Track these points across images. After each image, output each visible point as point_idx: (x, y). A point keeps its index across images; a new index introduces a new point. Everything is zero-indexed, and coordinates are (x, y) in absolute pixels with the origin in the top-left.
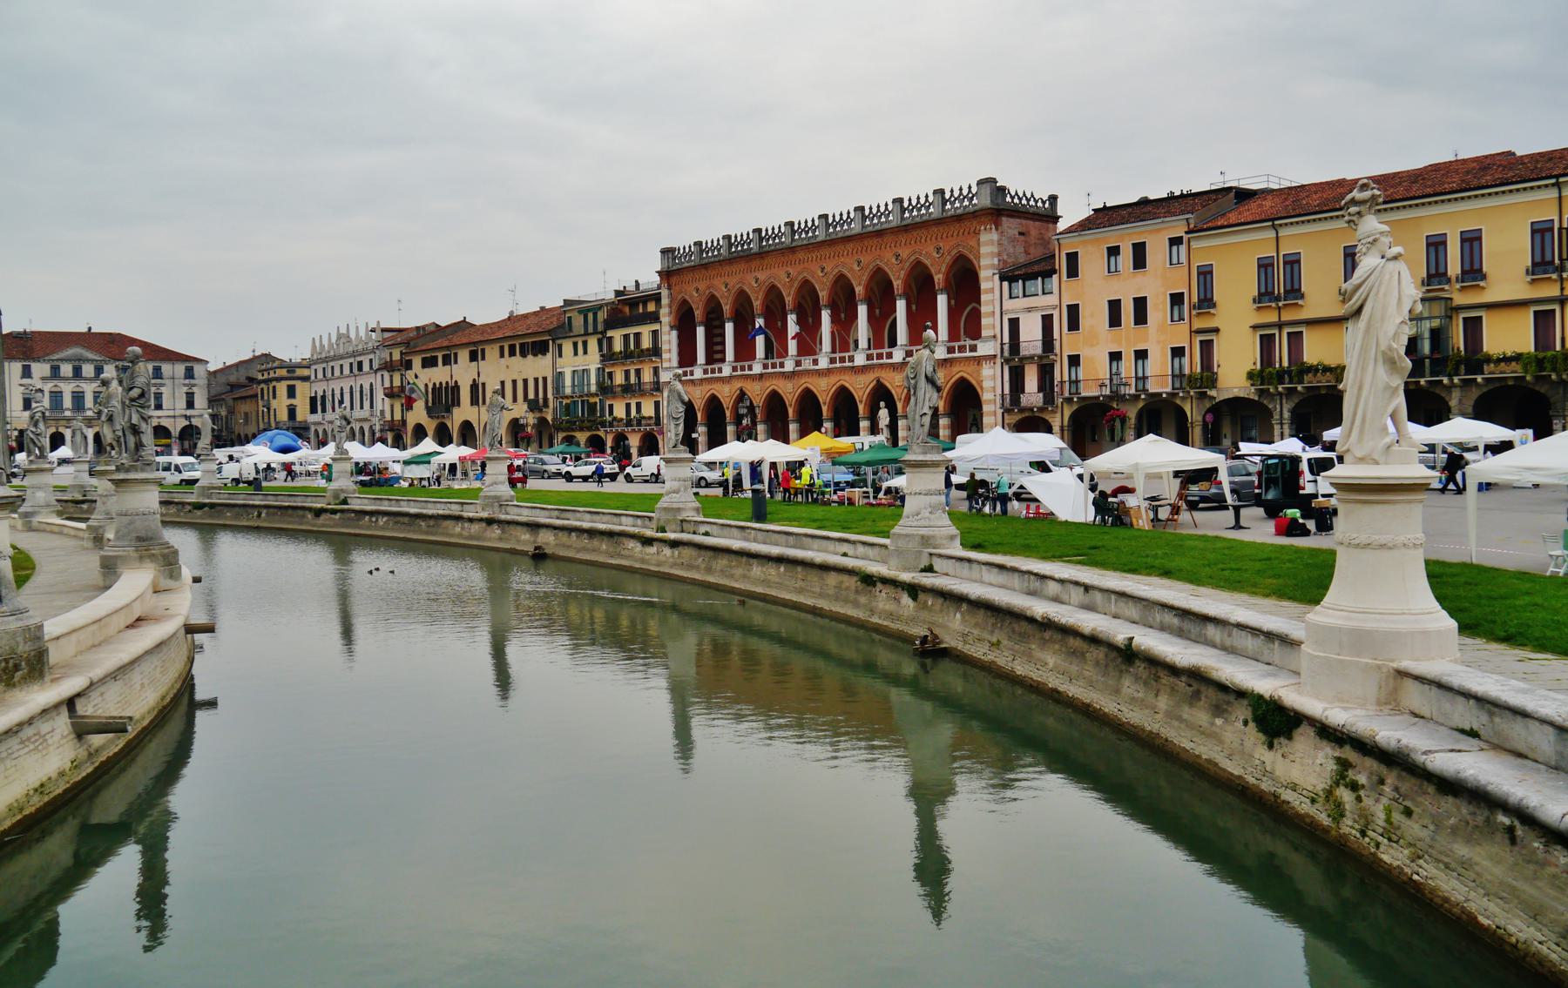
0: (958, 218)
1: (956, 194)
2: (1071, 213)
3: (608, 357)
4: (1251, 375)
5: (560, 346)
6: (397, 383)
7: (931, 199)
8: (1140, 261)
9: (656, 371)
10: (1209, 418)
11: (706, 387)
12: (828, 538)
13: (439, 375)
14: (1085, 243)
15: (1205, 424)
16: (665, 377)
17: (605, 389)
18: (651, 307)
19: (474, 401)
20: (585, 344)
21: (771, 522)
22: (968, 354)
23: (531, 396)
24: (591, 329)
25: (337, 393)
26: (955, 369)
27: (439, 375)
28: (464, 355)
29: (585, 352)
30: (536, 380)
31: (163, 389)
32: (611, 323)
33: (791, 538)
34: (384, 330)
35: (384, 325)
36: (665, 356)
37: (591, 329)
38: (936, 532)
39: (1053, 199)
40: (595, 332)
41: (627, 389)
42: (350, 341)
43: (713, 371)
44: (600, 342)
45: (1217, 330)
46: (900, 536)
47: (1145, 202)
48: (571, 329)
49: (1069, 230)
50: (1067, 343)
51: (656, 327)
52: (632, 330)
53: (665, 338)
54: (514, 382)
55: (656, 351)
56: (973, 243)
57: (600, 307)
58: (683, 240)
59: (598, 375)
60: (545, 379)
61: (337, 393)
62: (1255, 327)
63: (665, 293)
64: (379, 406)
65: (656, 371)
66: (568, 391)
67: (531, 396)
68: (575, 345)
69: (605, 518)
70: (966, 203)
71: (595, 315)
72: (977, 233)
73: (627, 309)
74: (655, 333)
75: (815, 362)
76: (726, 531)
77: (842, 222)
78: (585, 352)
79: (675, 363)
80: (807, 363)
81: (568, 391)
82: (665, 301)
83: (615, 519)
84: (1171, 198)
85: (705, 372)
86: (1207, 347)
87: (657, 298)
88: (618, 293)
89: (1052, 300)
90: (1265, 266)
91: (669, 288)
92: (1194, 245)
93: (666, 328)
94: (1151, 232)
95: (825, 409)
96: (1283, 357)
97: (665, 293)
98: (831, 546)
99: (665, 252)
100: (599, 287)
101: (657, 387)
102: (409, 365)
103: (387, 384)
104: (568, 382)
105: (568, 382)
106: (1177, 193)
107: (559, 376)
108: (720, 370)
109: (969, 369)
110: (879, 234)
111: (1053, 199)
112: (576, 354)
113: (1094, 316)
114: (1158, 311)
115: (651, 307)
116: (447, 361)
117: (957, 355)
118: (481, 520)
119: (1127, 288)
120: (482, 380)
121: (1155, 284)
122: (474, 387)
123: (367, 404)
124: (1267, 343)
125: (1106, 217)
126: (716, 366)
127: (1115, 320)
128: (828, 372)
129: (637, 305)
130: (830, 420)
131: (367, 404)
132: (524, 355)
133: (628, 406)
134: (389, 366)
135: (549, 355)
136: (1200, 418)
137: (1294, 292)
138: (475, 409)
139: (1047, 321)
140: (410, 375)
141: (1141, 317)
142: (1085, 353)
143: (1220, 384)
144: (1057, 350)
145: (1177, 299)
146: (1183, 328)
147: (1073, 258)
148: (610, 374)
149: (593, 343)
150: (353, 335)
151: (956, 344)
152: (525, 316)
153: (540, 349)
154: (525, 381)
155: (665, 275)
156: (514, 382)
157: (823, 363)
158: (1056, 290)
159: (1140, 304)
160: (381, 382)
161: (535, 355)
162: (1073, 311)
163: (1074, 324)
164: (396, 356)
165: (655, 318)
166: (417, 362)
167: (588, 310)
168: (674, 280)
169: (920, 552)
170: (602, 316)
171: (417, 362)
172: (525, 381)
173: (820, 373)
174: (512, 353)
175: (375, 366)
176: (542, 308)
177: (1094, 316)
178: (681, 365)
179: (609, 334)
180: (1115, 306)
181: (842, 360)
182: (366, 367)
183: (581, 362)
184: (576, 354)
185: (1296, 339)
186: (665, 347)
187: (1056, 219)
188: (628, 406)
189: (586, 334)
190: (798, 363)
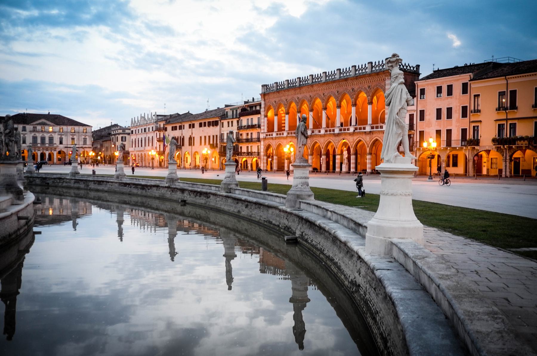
0: (377, 74)
1: (377, 64)
2: (424, 72)
3: (240, 128)
4: (494, 140)
5: (223, 123)
6: (162, 136)
7: (367, 66)
8: (450, 92)
9: (259, 133)
10: (476, 158)
11: (277, 141)
12: (272, 195)
13: (177, 133)
14: (428, 85)
15: (474, 161)
16: (262, 136)
17: (239, 140)
18: (258, 108)
19: (190, 144)
20: (232, 122)
21: (269, 191)
22: (379, 129)
23: (211, 142)
24: (235, 117)
25: (140, 140)
26: (374, 135)
27: (177, 133)
28: (187, 125)
29: (232, 126)
30: (213, 136)
31: (63, 136)
32: (242, 115)
33: (262, 196)
34: (158, 116)
35: (157, 114)
36: (262, 128)
37: (235, 117)
38: (303, 193)
39: (418, 66)
40: (236, 118)
41: (247, 141)
42: (145, 119)
43: (280, 134)
44: (238, 122)
45: (481, 121)
46: (289, 194)
47: (456, 68)
48: (227, 117)
49: (422, 79)
50: (419, 126)
51: (259, 116)
52: (250, 117)
53: (262, 120)
54: (205, 137)
55: (259, 126)
56: (383, 84)
57: (239, 108)
58: (270, 82)
59: (236, 135)
60: (217, 136)
61: (140, 140)
62: (496, 120)
63: (263, 103)
64: (155, 145)
65: (259, 133)
66: (225, 141)
67: (211, 142)
68: (228, 122)
69: (207, 187)
70: (381, 68)
71: (236, 111)
72: (384, 80)
73: (249, 109)
74: (259, 118)
75: (320, 132)
76: (244, 193)
77: (332, 75)
78: (232, 126)
79: (266, 131)
80: (316, 132)
81: (225, 141)
82: (263, 106)
83: (210, 188)
84: (466, 66)
85: (277, 134)
86: (476, 130)
87: (260, 105)
88: (245, 102)
89: (414, 108)
90: (502, 94)
91: (265, 101)
92: (472, 86)
93: (263, 117)
94: (455, 80)
95: (322, 150)
96: (507, 133)
97: (263, 103)
98: (273, 198)
99: (263, 86)
100: (238, 101)
101: (259, 140)
102: (166, 129)
103: (158, 137)
104: (225, 137)
105: (225, 137)
106: (468, 64)
107: (222, 135)
108: (283, 134)
109: (379, 136)
110: (346, 80)
111: (418, 66)
112: (229, 126)
113: (430, 115)
114: (457, 114)
115: (258, 108)
116: (180, 128)
117: (375, 130)
118: (166, 187)
119: (444, 103)
120: (193, 136)
121: (456, 102)
122: (190, 138)
123: (151, 144)
124: (501, 128)
125: (438, 74)
126: (281, 132)
127: (439, 117)
128: (324, 136)
129: (253, 107)
130: (324, 155)
131: (151, 144)
132: (209, 126)
133: (248, 147)
134: (158, 129)
135: (219, 127)
136: (472, 158)
137: (513, 106)
138: (190, 147)
139: (411, 117)
140: (167, 133)
141: (449, 116)
142: (426, 130)
143: (480, 144)
144: (415, 129)
145: (464, 109)
146: (467, 120)
147: (423, 92)
148: (241, 135)
149: (235, 121)
150: (146, 118)
151: (375, 125)
152: (211, 111)
153: (215, 124)
154: (209, 137)
155: (264, 95)
156: (205, 137)
157: (323, 132)
158: (415, 104)
159: (449, 110)
160: (155, 135)
161: (213, 126)
162: (422, 113)
163: (422, 118)
164: (162, 126)
165: (258, 112)
166: (169, 128)
167: (234, 109)
168: (266, 97)
169: (296, 201)
170: (239, 111)
171: (169, 128)
172: (209, 137)
173: (321, 136)
174: (205, 126)
175: (154, 129)
176: (218, 108)
177: (430, 115)
178: (268, 131)
179: (241, 118)
180: (439, 111)
181: (330, 131)
182: (151, 130)
183: (230, 129)
184: (229, 126)
185: (513, 127)
186: (262, 124)
187: (419, 74)
188: (248, 147)
189: (233, 118)
190: (313, 132)
